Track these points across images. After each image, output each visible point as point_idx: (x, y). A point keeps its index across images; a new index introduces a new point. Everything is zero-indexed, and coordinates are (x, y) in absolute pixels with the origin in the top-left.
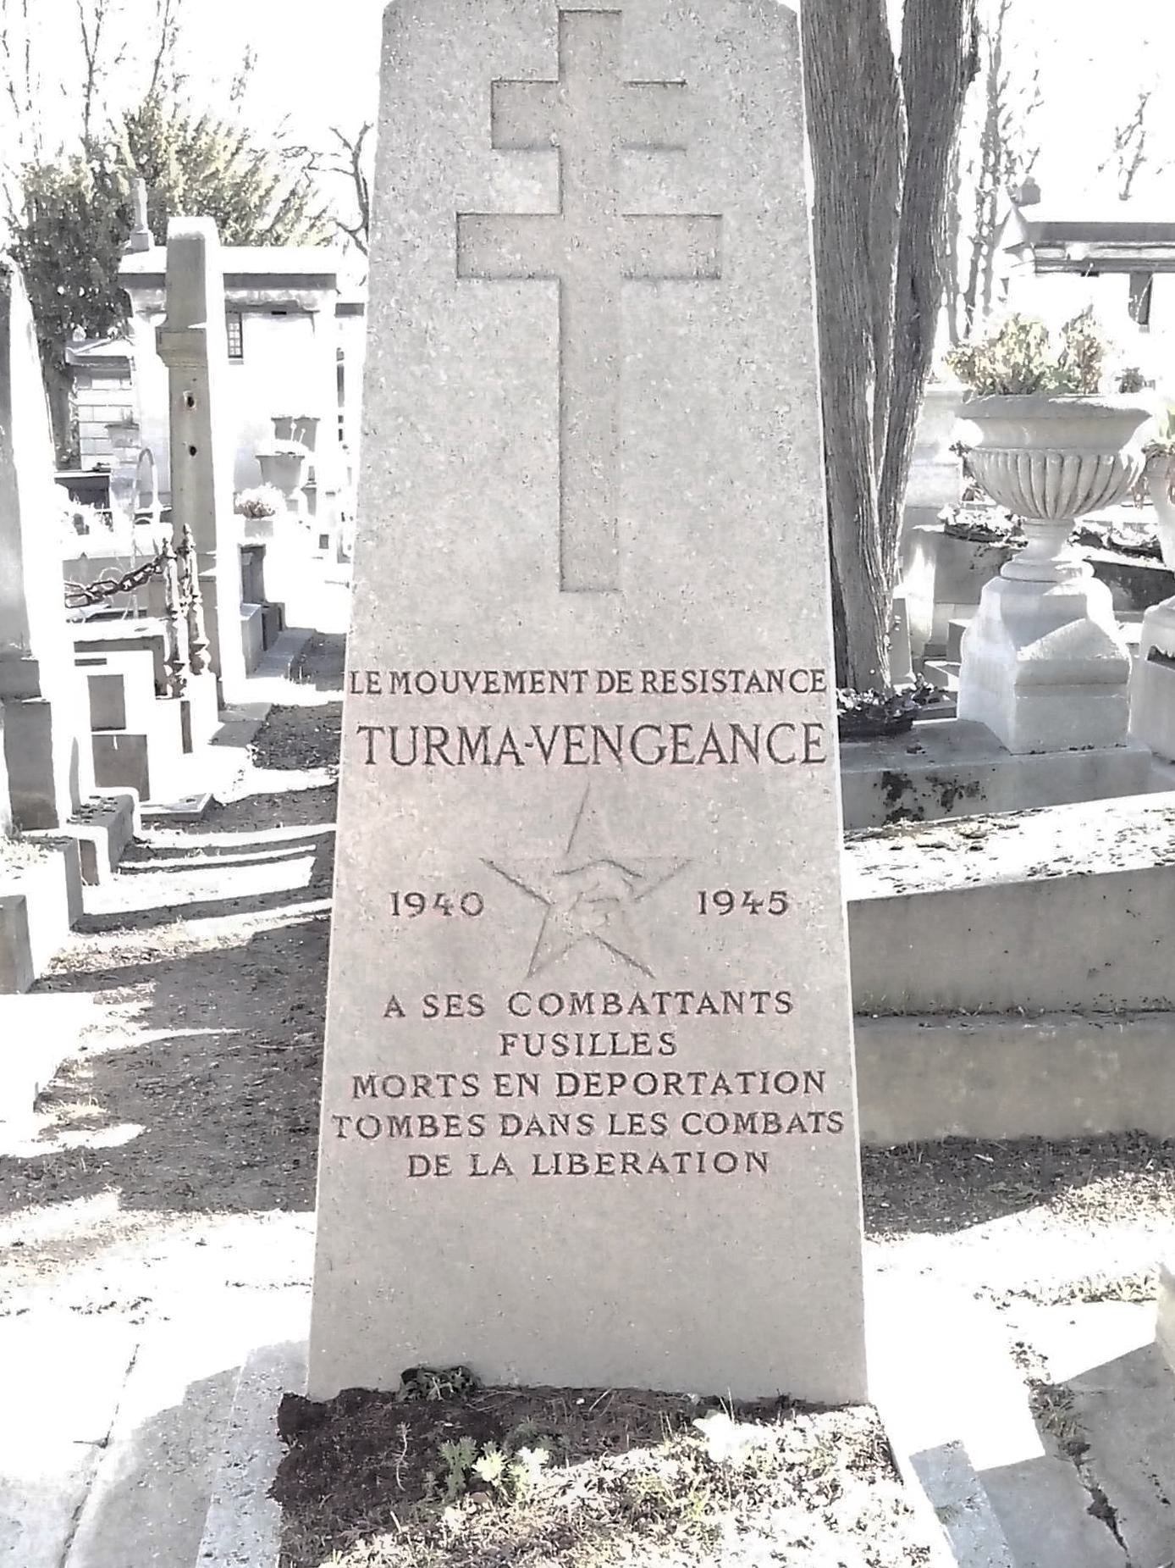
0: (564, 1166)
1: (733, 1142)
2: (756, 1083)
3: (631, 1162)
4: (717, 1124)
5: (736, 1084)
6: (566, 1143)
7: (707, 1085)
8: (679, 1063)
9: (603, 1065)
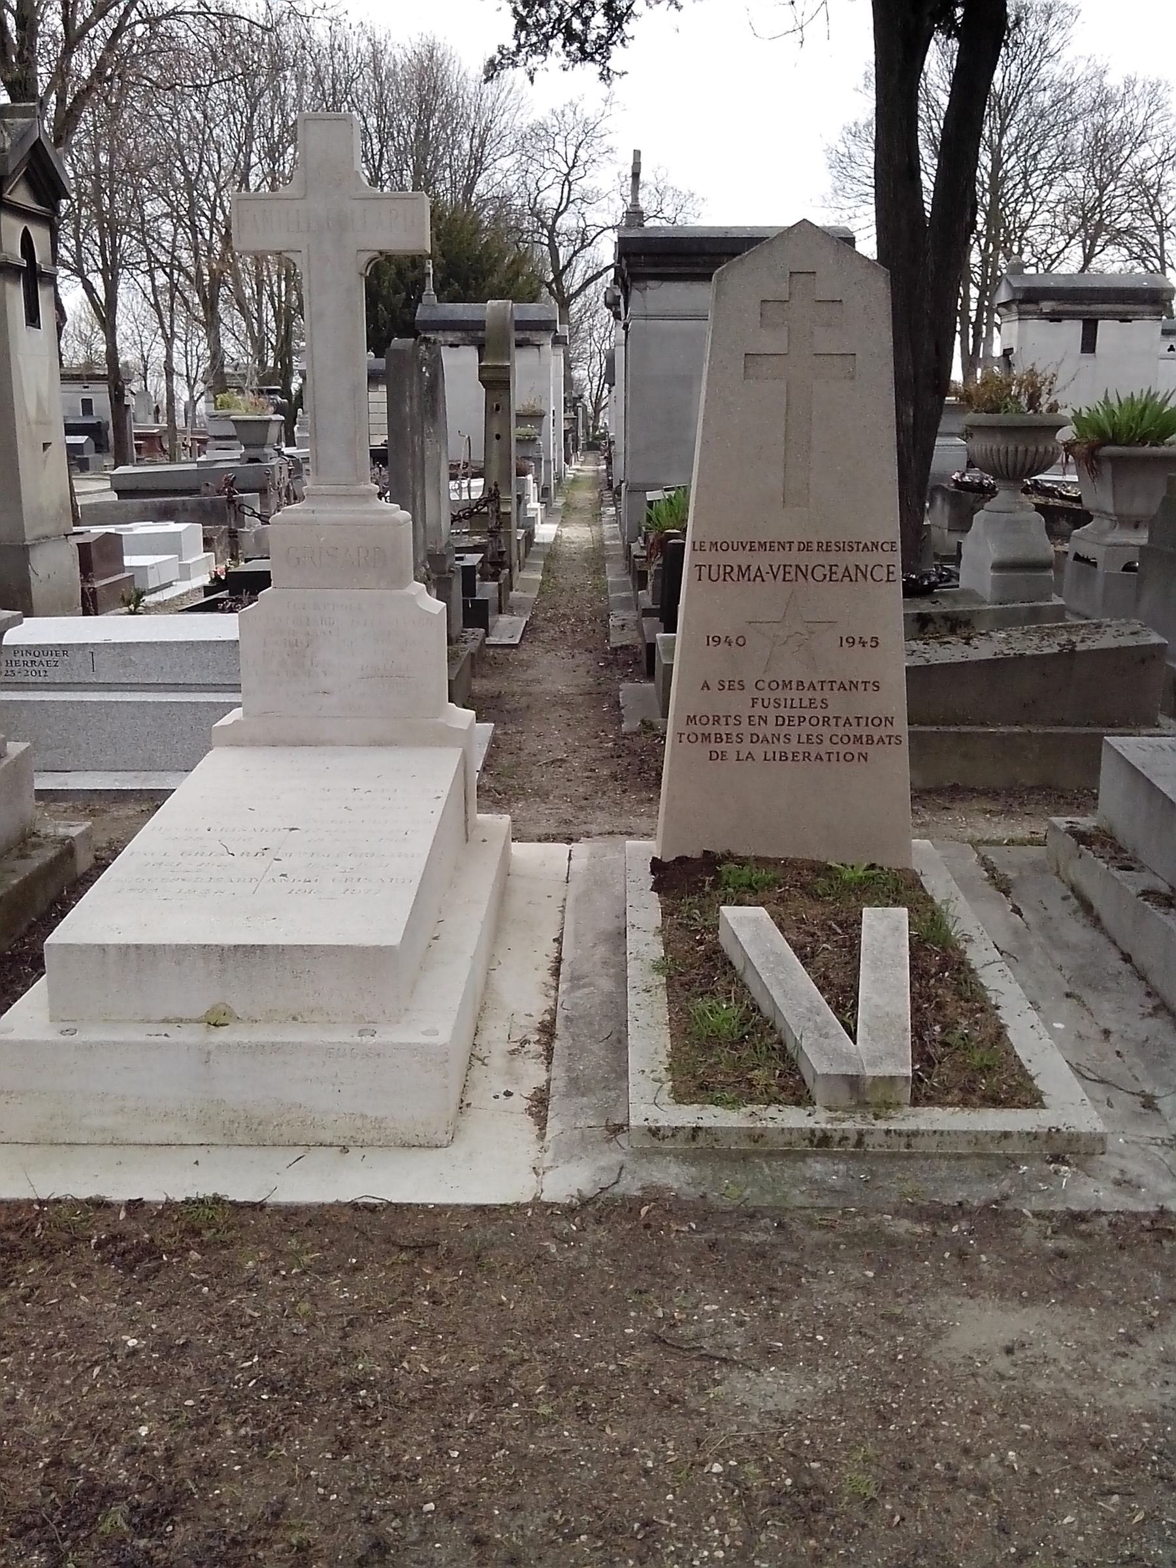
0: (777, 756)
1: (855, 749)
2: (863, 722)
3: (807, 756)
4: (845, 740)
5: (854, 722)
6: (780, 747)
7: (841, 722)
8: (830, 712)
9: (796, 713)
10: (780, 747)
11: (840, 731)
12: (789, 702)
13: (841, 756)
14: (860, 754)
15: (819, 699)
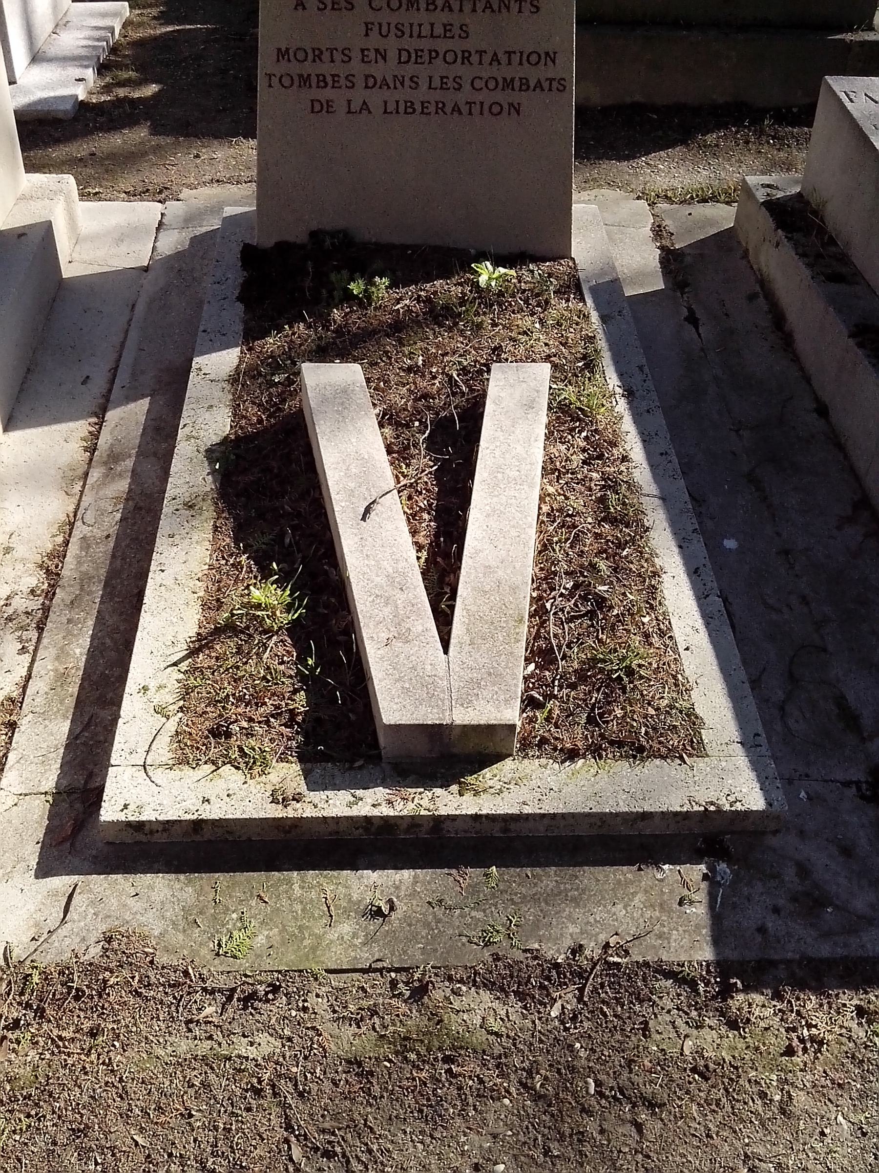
0: (402, 109)
1: (503, 97)
2: (516, 58)
3: (441, 107)
4: (492, 85)
5: (504, 59)
6: (402, 94)
7: (487, 58)
8: (470, 44)
9: (425, 44)
10: (402, 94)
11: (486, 72)
12: (416, 29)
13: (486, 107)
14: (511, 105)
15: (457, 25)
